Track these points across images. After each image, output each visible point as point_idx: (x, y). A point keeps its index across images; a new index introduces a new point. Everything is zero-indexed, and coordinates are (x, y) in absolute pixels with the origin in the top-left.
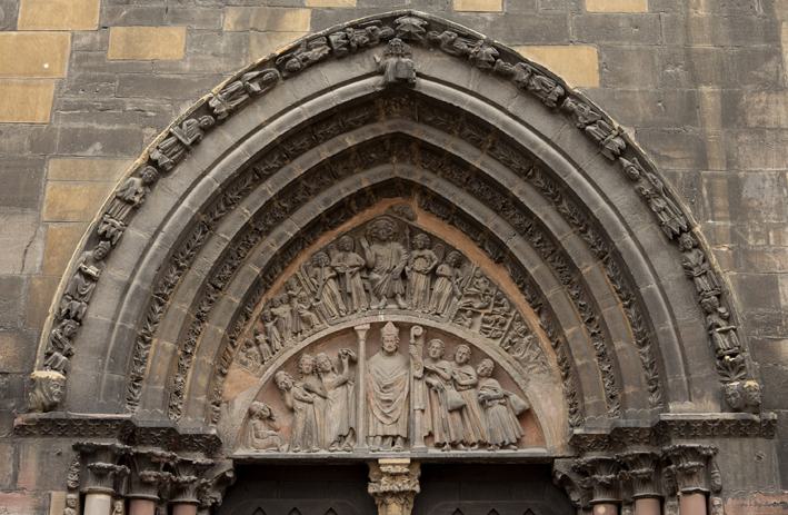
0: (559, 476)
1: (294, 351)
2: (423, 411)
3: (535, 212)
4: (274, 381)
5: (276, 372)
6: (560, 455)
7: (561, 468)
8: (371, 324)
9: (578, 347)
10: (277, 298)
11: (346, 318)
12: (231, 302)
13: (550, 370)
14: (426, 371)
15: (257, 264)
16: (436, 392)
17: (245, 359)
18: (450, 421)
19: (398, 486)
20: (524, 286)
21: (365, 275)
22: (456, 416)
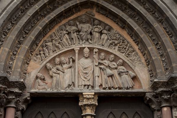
0: (148, 99)
1: (53, 56)
2: (98, 77)
3: (137, 8)
4: (45, 67)
5: (46, 64)
6: (148, 91)
7: (148, 96)
8: (80, 48)
9: (153, 53)
10: (47, 40)
11: (71, 46)
12: (31, 38)
13: (142, 63)
14: (100, 63)
15: (40, 26)
16: (103, 70)
17: (35, 59)
18: (108, 80)
19: (89, 102)
20: (132, 35)
21: (78, 34)
22: (110, 78)
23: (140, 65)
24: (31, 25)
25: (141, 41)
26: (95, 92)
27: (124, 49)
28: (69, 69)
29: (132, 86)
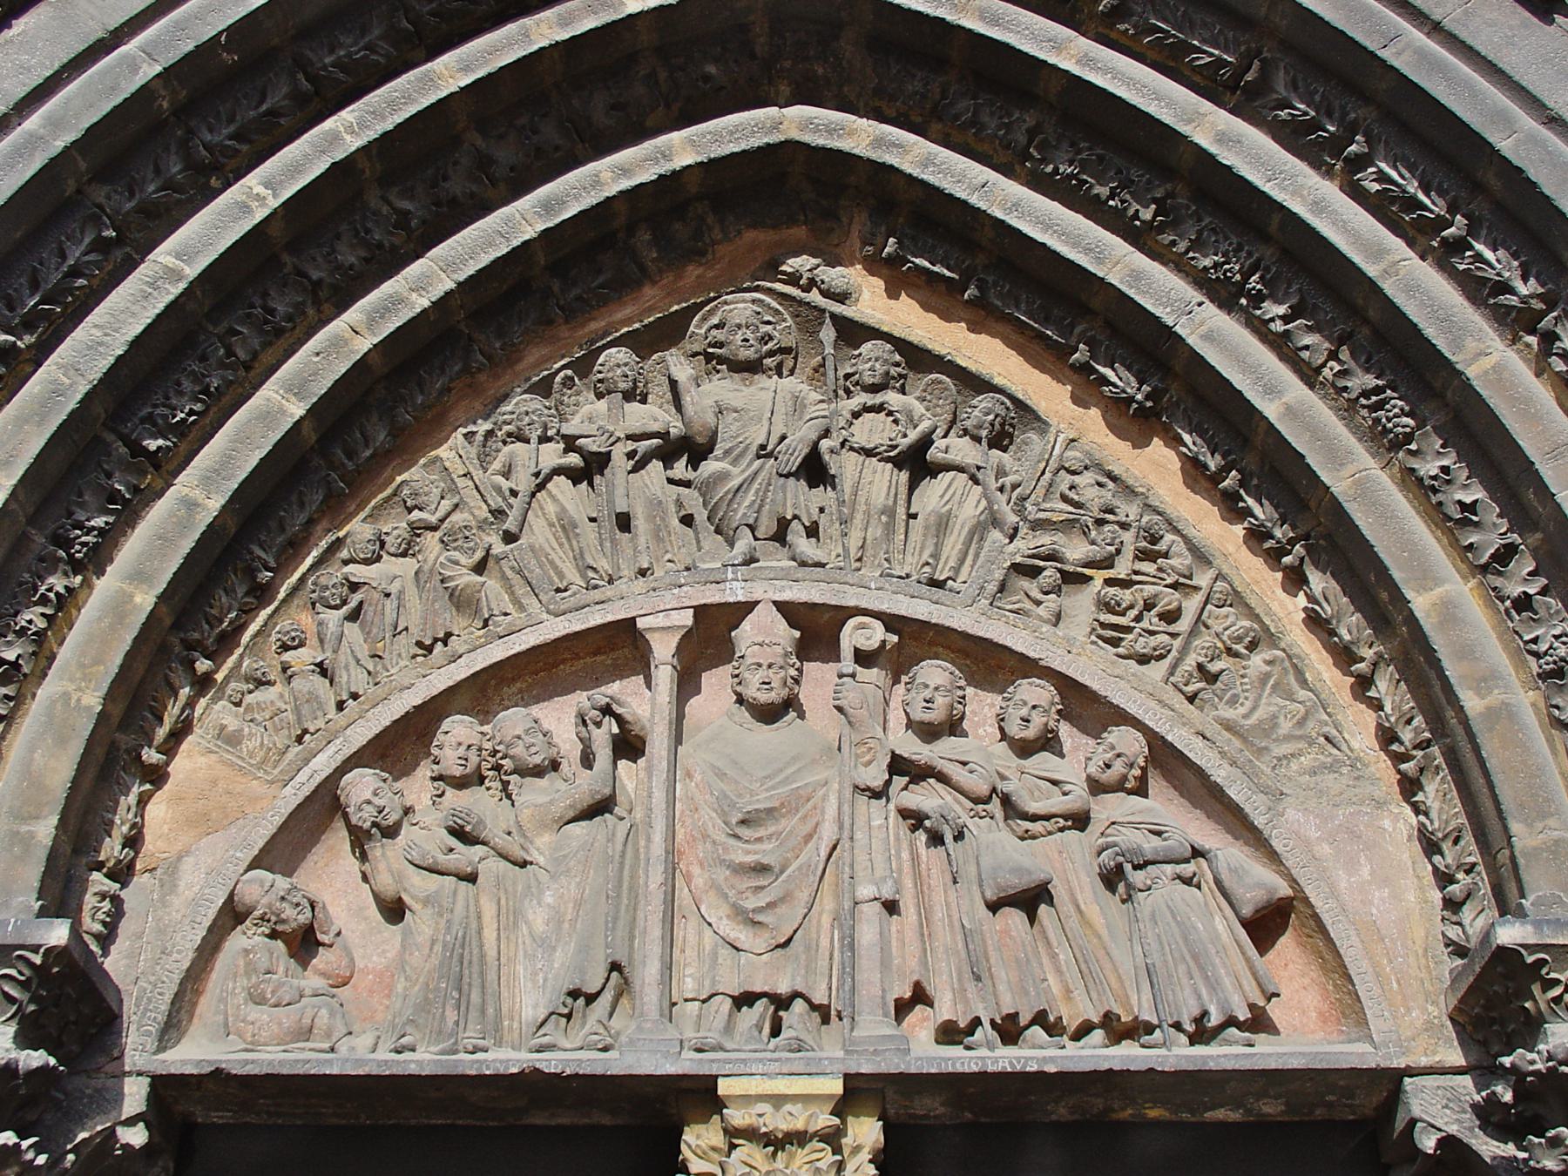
0: (1428, 1143)
2: (891, 907)
6: (1424, 1061)
8: (701, 611)
9: (1466, 652)
11: (609, 591)
13: (1355, 763)
14: (898, 765)
21: (680, 469)
24: (197, 378)
25: (1328, 537)
27: (1151, 620)
29: (1252, 1007)
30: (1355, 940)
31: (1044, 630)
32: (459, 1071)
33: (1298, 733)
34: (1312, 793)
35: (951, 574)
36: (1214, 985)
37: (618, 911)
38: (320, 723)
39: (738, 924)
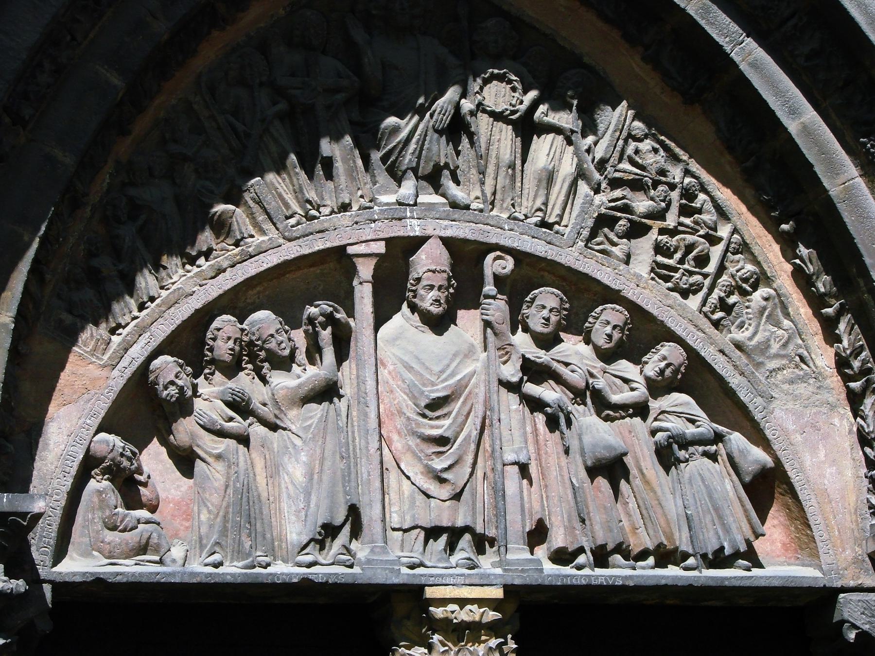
0: (852, 635)
2: (524, 469)
6: (852, 584)
8: (389, 241)
13: (818, 376)
22: (602, 482)
23: (801, 389)
26: (509, 582)
28: (316, 410)
29: (749, 543)
30: (814, 501)
31: (621, 268)
32: (260, 580)
33: (782, 352)
34: (791, 397)
35: (557, 219)
36: (727, 530)
37: (350, 468)
38: (127, 318)
39: (429, 479)
